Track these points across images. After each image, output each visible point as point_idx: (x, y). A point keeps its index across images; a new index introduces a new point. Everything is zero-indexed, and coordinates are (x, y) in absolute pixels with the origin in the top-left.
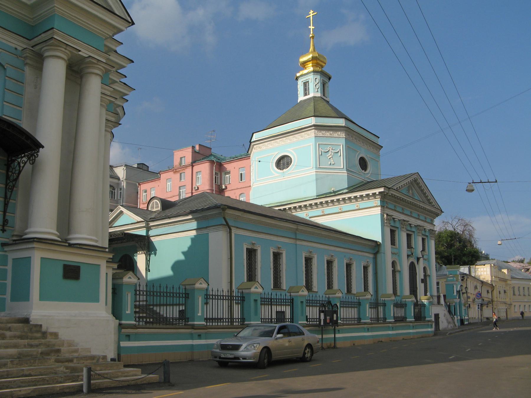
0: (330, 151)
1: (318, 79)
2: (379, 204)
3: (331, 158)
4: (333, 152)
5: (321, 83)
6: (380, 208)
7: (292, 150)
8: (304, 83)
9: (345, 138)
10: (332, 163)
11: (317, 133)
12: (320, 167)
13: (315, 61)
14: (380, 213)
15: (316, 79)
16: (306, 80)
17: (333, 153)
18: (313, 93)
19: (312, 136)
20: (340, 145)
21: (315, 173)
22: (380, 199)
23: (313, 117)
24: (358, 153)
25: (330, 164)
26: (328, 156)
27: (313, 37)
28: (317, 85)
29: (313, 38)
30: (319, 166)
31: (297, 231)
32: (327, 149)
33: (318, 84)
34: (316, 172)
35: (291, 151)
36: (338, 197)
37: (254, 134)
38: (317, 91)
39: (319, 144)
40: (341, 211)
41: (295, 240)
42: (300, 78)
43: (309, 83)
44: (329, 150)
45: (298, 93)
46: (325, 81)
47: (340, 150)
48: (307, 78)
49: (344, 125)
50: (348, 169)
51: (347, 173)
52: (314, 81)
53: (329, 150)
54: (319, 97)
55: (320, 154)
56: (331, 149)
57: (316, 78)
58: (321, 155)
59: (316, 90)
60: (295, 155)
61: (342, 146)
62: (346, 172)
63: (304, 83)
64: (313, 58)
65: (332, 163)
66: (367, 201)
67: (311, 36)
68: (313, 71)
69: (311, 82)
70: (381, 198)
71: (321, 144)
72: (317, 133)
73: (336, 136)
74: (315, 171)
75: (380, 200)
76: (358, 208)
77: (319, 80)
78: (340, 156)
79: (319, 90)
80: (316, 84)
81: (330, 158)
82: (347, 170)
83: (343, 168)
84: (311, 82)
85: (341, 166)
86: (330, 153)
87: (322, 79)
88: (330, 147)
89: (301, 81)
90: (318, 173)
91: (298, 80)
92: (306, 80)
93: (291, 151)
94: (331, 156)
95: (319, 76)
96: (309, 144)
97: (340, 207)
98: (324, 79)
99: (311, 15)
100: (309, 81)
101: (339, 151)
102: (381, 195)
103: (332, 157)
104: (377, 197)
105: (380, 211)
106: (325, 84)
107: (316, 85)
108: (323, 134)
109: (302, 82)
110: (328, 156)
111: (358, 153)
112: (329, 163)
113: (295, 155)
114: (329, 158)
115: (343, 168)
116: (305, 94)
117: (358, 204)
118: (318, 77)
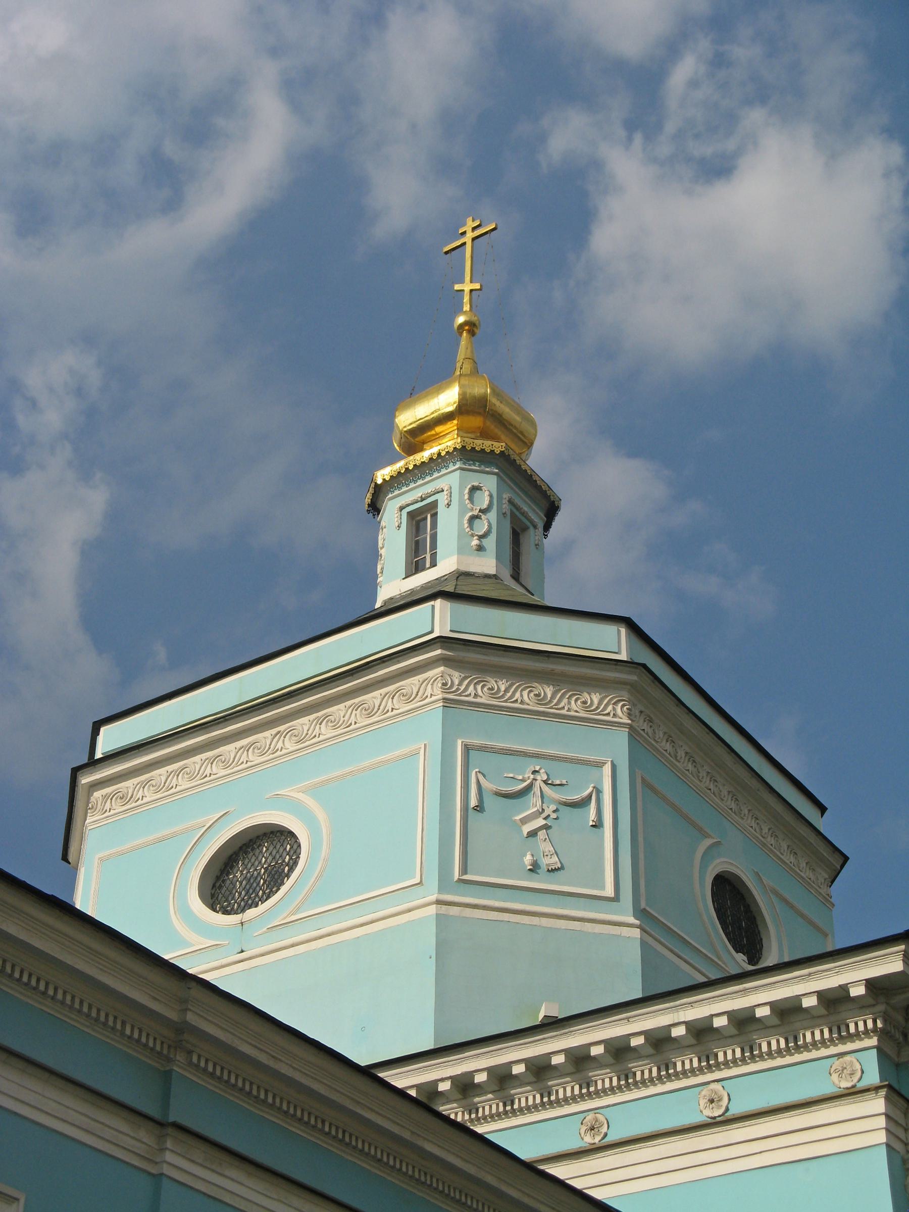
0: (536, 789)
1: (487, 493)
2: (873, 1077)
3: (542, 834)
4: (554, 801)
5: (502, 515)
6: (878, 1104)
7: (311, 790)
8: (411, 515)
9: (631, 727)
10: (545, 862)
11: (460, 684)
12: (465, 877)
13: (476, 421)
14: (881, 1137)
15: (474, 489)
16: (422, 499)
17: (553, 807)
18: (456, 556)
19: (428, 700)
20: (600, 765)
21: (432, 909)
22: (874, 1041)
23: (438, 603)
24: (708, 842)
25: (535, 868)
26: (524, 821)
27: (471, 327)
28: (477, 521)
29: (472, 333)
30: (464, 870)
31: (180, 1057)
32: (520, 777)
33: (483, 517)
34: (439, 902)
35: (300, 796)
36: (575, 1039)
37: (102, 730)
38: (480, 548)
39: (467, 749)
40: (597, 1139)
41: (145, 1136)
42: (390, 495)
43: (436, 514)
44: (529, 788)
45: (379, 570)
46: (524, 514)
47: (598, 791)
48: (429, 489)
49: (623, 656)
50: (643, 905)
51: (643, 930)
52: (466, 496)
53: (529, 788)
54: (487, 576)
55: (473, 802)
56: (538, 783)
57: (476, 484)
58: (479, 808)
59: (475, 542)
60: (321, 815)
61: (607, 769)
62: (632, 920)
63: (411, 515)
64: (465, 408)
65: (545, 862)
66: (779, 1062)
67: (461, 319)
68: (464, 447)
69: (448, 505)
70: (883, 1035)
71: (483, 749)
72: (460, 684)
73: (572, 713)
74: (433, 898)
75: (879, 1048)
76: (717, 1113)
77: (491, 496)
78: (598, 825)
79: (490, 543)
80: (476, 513)
81: (533, 834)
82: (641, 913)
83: (616, 898)
84: (448, 505)
85: (603, 888)
86: (533, 803)
87: (506, 496)
88: (534, 772)
89: (398, 506)
90: (454, 911)
91: (378, 511)
92: (422, 499)
93: (300, 796)
94: (540, 822)
95: (495, 477)
96: (405, 750)
97: (590, 1117)
98: (518, 501)
99: (470, 235)
100: (434, 504)
101: (590, 796)
102: (881, 1008)
103: (546, 827)
104: (852, 1029)
105: (882, 1122)
106: (525, 529)
107: (473, 518)
108: (493, 693)
109: (402, 508)
110: (524, 821)
111: (708, 842)
112: (528, 859)
113: (321, 815)
114: (527, 829)
115: (616, 898)
116: (415, 566)
117: (713, 1086)
118: (489, 483)
